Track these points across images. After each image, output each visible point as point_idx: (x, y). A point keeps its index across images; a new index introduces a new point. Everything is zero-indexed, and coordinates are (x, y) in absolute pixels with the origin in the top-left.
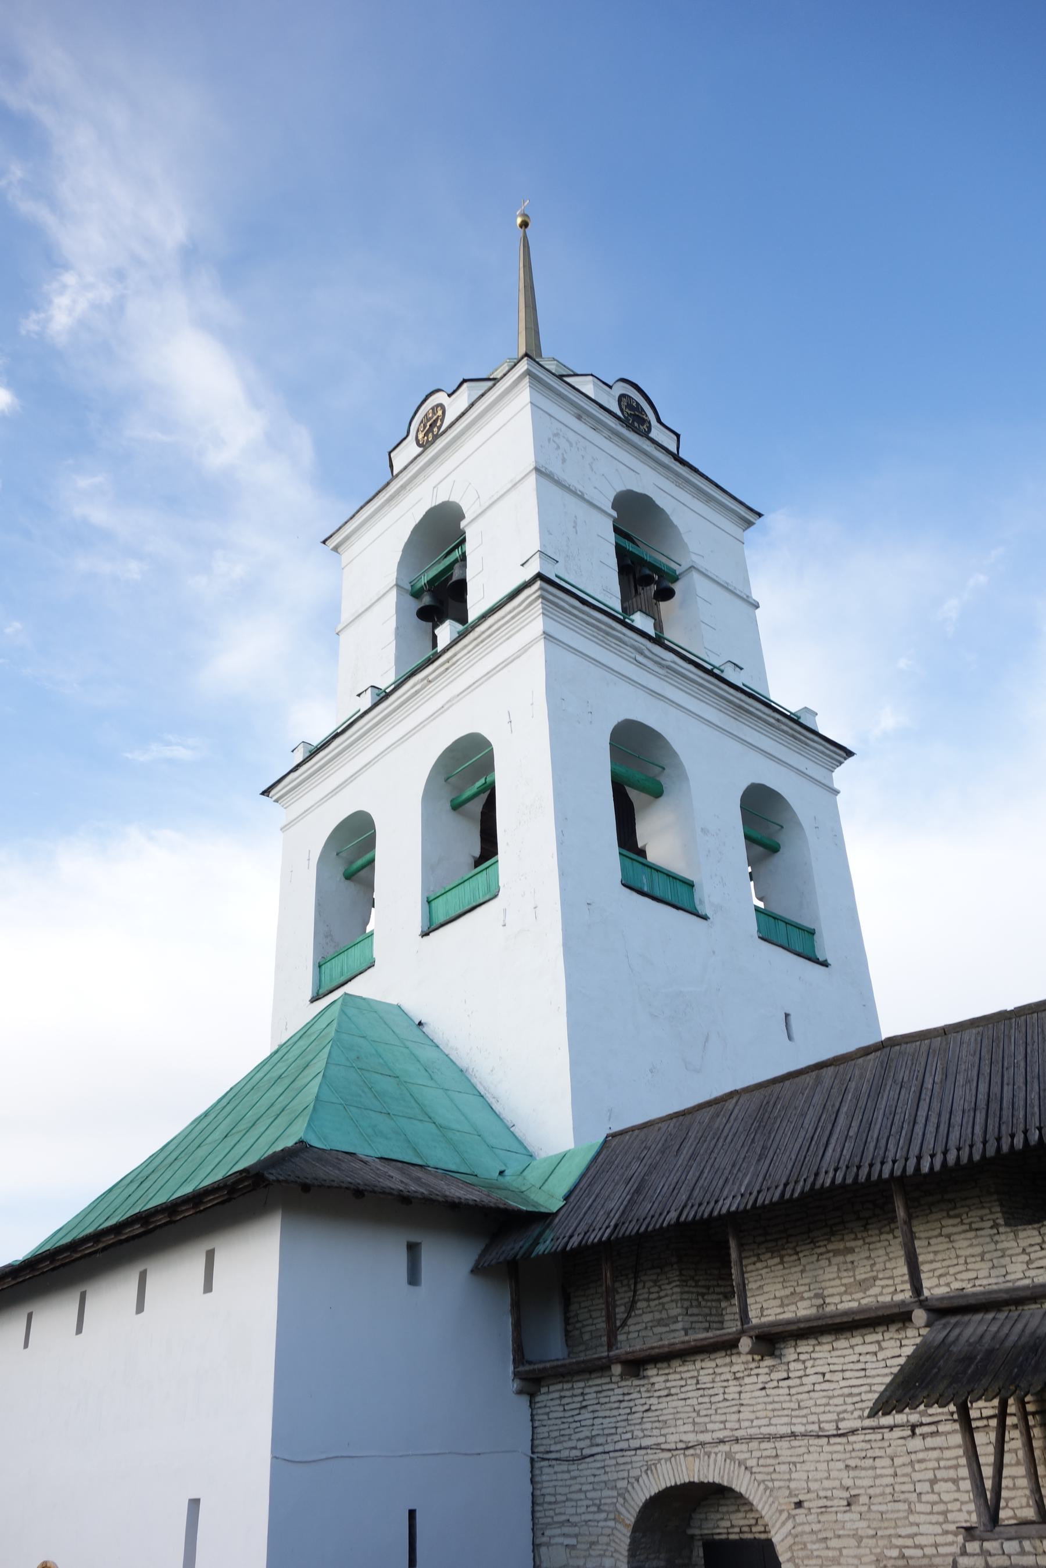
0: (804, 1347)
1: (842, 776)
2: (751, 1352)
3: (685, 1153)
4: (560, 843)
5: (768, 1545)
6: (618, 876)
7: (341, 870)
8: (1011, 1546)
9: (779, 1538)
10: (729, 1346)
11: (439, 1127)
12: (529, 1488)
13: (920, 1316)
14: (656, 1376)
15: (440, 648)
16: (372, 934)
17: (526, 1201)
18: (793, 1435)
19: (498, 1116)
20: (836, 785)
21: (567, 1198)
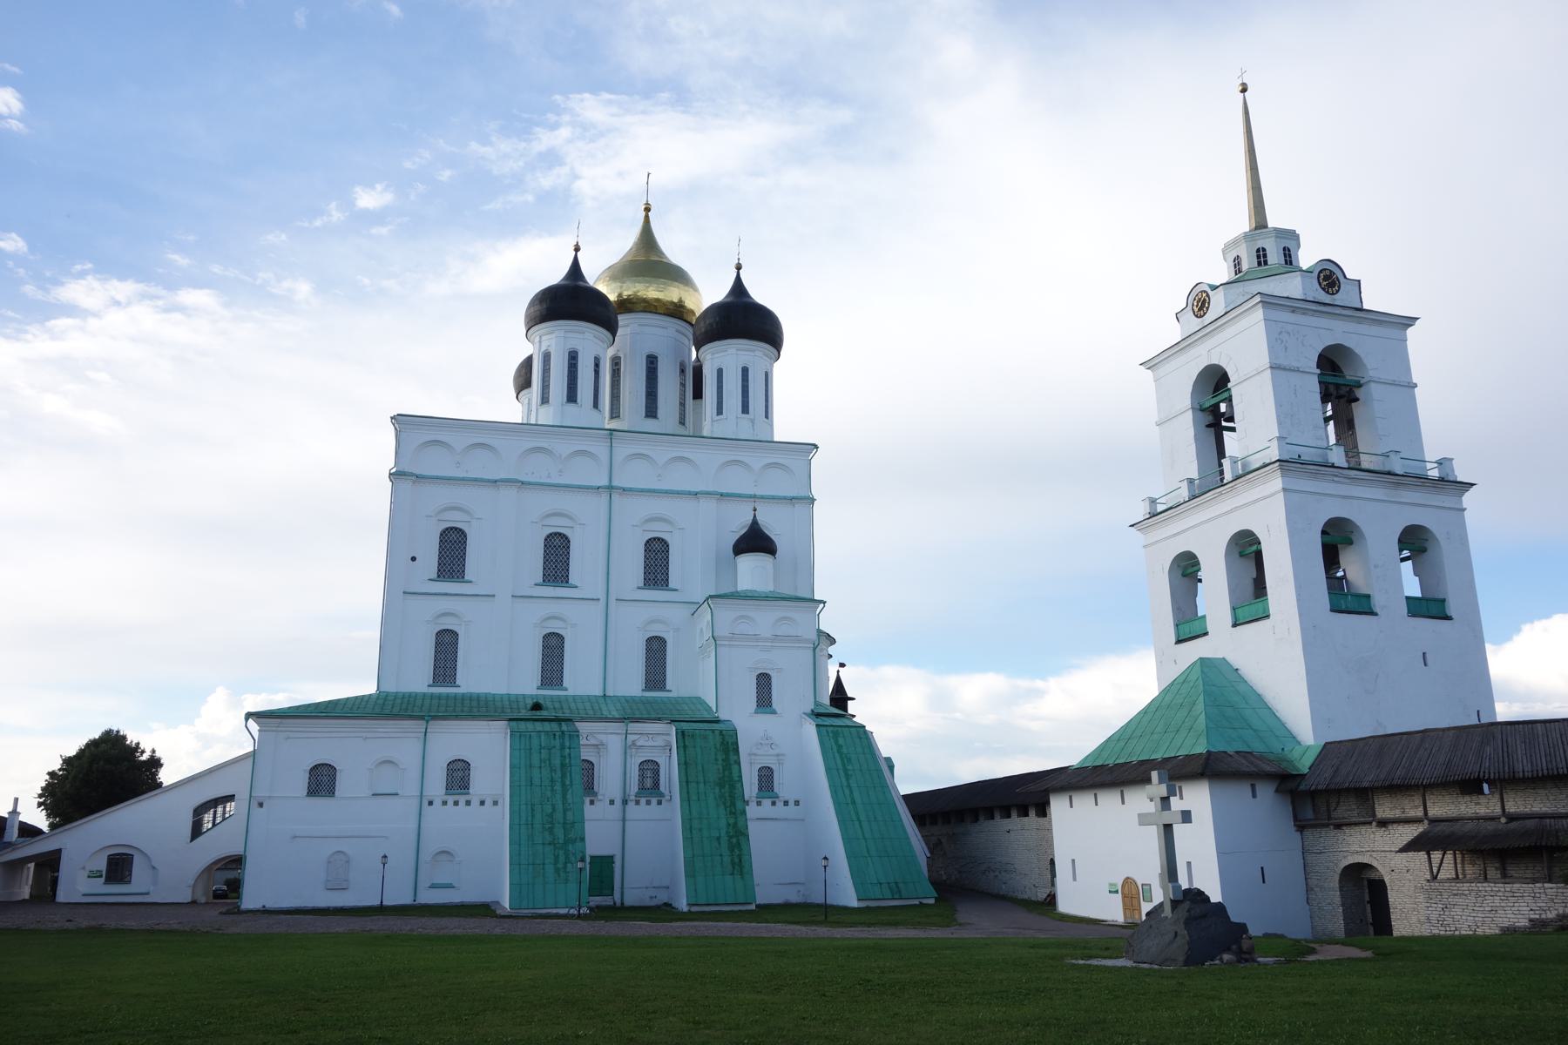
0: (1395, 826)
1: (1468, 499)
2: (1377, 826)
3: (1353, 759)
4: (1298, 600)
5: (1383, 882)
6: (1328, 607)
7: (1181, 572)
8: (1437, 884)
9: (1387, 879)
10: (1370, 823)
11: (1255, 731)
12: (1302, 861)
13: (1426, 822)
14: (1347, 830)
15: (1225, 481)
16: (1204, 617)
17: (1294, 766)
18: (1391, 851)
19: (1278, 718)
20: (1464, 506)
21: (1310, 768)
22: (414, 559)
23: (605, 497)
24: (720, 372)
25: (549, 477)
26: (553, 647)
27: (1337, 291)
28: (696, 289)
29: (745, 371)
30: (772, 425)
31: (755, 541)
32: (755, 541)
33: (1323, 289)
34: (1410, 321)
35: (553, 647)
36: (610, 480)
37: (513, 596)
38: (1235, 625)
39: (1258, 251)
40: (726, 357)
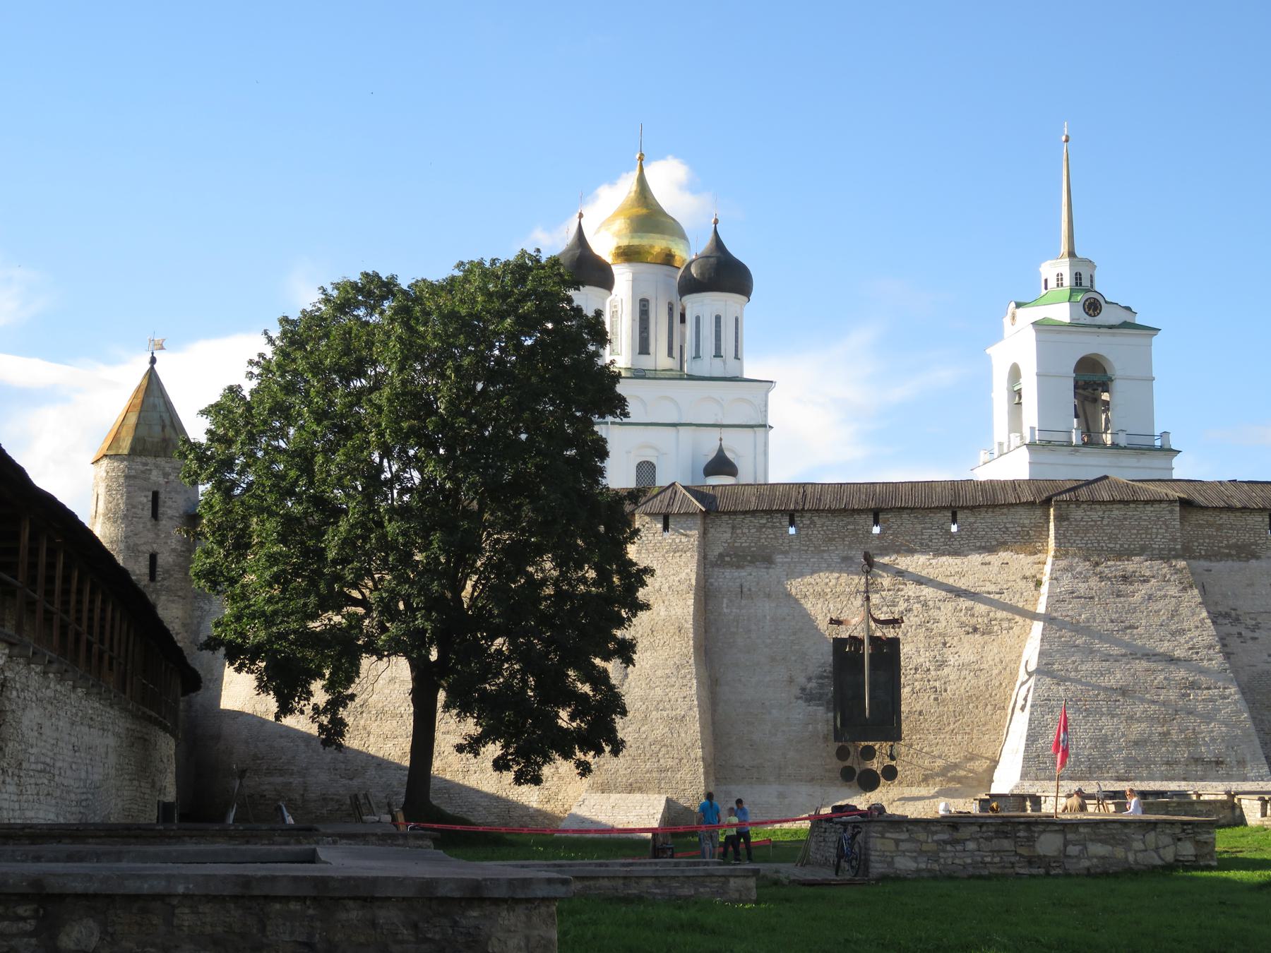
24: (698, 319)
27: (1098, 314)
29: (718, 319)
33: (1087, 313)
39: (1058, 275)
40: (704, 305)
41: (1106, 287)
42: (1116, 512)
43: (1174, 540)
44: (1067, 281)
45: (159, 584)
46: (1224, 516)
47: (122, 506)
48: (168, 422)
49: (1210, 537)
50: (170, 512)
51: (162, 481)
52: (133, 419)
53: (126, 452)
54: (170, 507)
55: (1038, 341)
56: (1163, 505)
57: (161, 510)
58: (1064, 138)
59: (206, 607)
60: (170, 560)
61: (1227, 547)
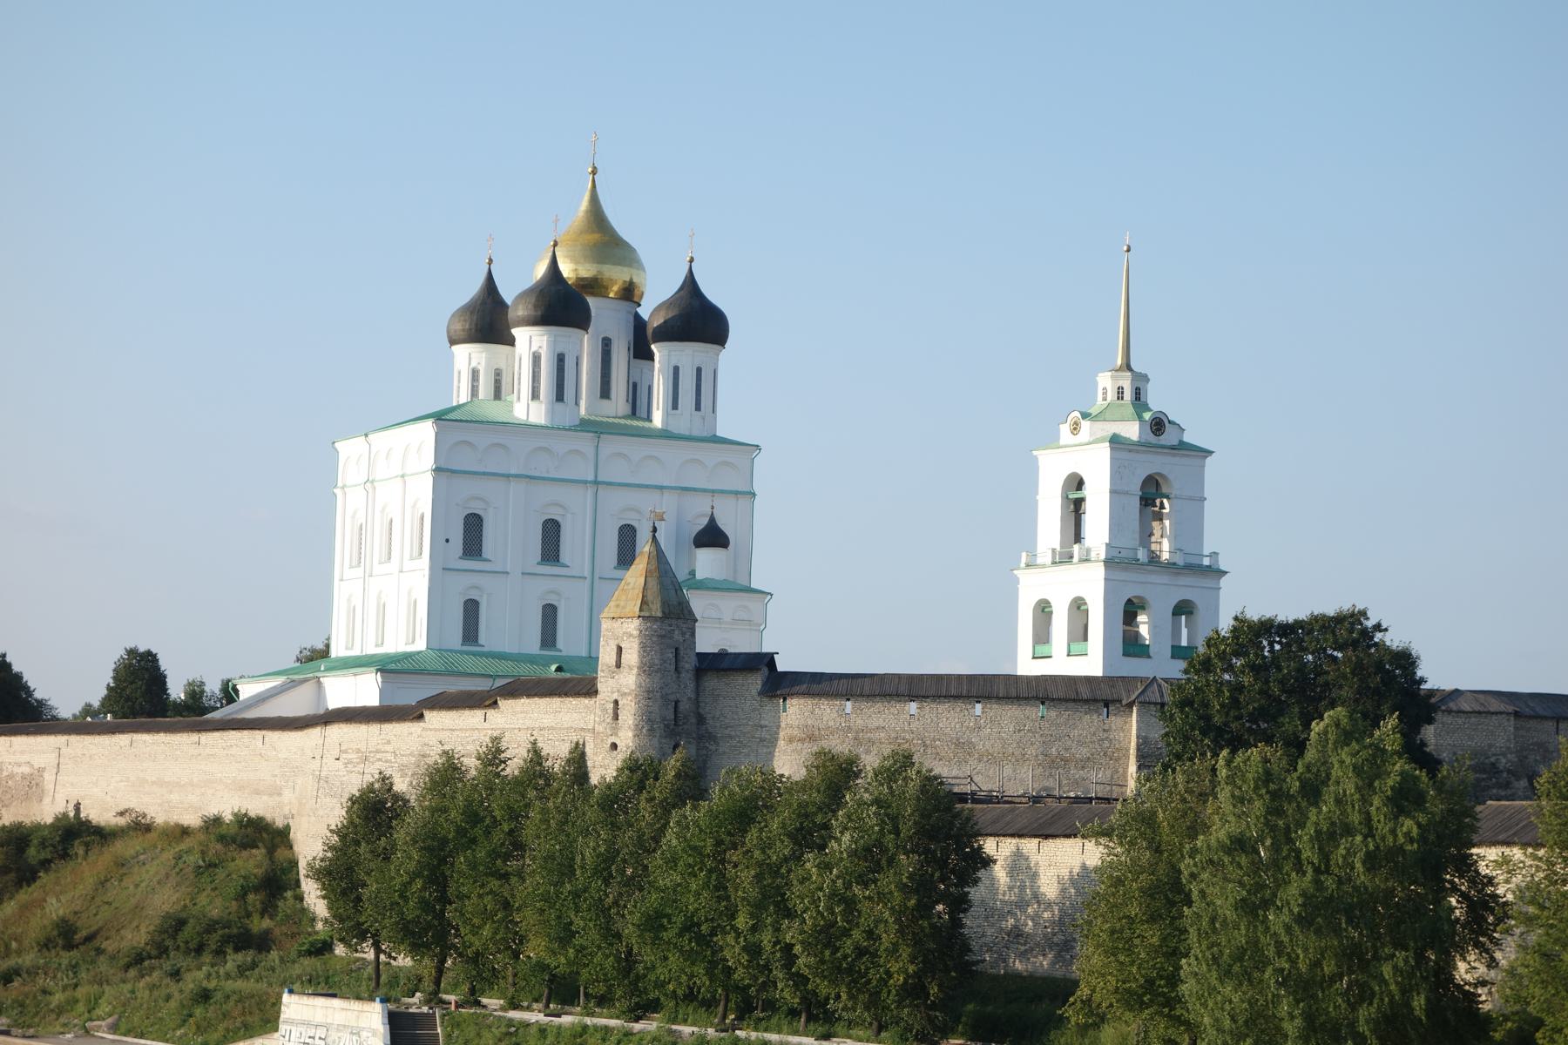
22: (447, 541)
23: (590, 492)
25: (548, 472)
26: (550, 614)
28: (644, 270)
29: (699, 370)
30: (716, 418)
31: (712, 536)
32: (712, 536)
33: (1153, 432)
34: (1211, 453)
35: (550, 614)
36: (596, 477)
37: (523, 574)
38: (1068, 655)
39: (1119, 388)
41: (1157, 401)
42: (1473, 719)
43: (1509, 740)
44: (1128, 395)
45: (681, 728)
46: (1531, 722)
47: (657, 662)
48: (677, 587)
49: (1522, 736)
50: (687, 666)
51: (681, 639)
52: (653, 583)
53: (659, 614)
54: (687, 662)
55: (1112, 459)
56: (1503, 716)
57: (681, 664)
58: (1125, 248)
59: (713, 748)
60: (687, 707)
61: (1532, 744)
